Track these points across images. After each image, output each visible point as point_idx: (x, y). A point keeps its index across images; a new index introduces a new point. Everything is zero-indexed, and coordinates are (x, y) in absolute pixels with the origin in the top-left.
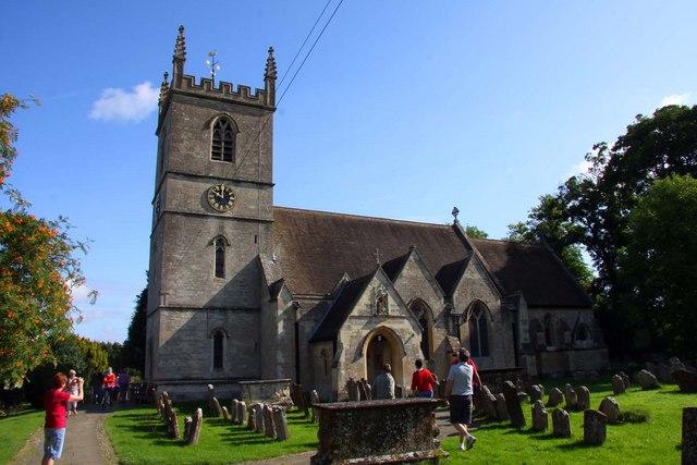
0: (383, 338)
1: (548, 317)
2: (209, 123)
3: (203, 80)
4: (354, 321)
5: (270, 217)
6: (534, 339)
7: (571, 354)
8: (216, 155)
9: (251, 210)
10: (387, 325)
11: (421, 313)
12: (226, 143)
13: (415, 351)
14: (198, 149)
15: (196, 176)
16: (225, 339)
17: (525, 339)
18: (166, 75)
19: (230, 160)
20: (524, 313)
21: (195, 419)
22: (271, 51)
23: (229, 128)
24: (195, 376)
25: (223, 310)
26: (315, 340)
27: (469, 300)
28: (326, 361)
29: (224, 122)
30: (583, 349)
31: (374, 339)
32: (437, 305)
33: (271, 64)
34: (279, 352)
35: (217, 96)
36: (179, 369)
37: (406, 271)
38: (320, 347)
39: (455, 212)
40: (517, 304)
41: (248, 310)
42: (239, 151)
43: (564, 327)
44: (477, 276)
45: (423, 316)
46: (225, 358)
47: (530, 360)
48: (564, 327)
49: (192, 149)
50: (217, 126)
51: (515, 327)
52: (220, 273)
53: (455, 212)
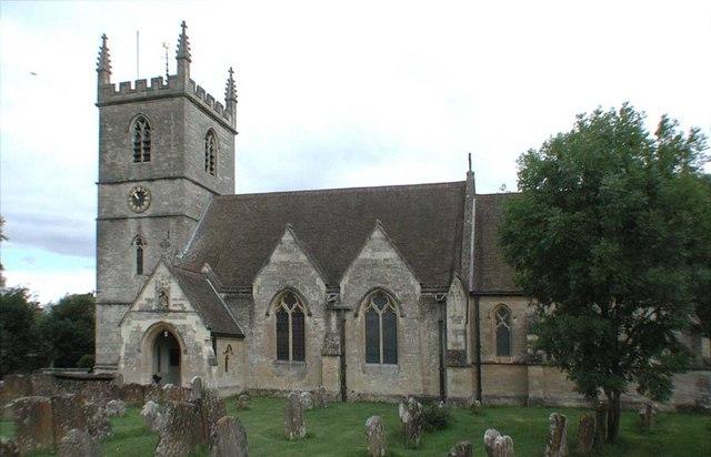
8: (137, 157)
9: (164, 206)
10: (168, 321)
27: (365, 287)
32: (315, 292)
36: (110, 356)
42: (154, 149)
44: (390, 254)
45: (297, 308)
51: (442, 325)
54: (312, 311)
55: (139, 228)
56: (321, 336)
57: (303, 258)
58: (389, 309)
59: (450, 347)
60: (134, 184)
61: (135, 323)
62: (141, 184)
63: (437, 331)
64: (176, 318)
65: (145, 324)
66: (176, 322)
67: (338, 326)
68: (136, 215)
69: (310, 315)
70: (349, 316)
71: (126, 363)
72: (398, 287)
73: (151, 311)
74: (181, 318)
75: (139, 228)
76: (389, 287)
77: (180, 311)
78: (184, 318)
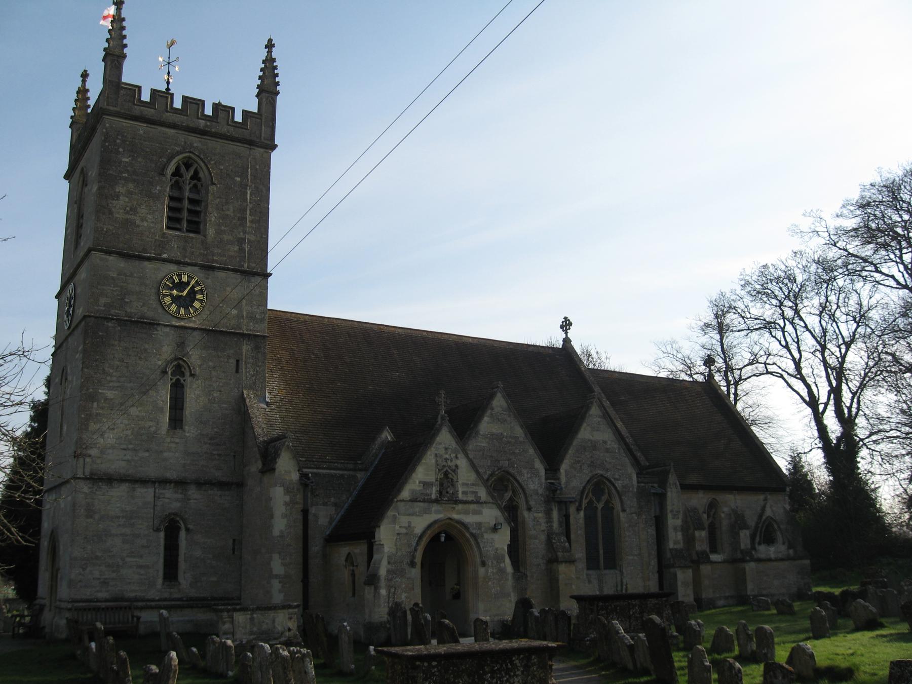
0: (449, 537)
1: (712, 506)
2: (165, 167)
3: (154, 92)
4: (401, 505)
5: (262, 329)
6: (689, 540)
7: (750, 566)
8: (174, 221)
10: (456, 516)
11: (508, 495)
12: (191, 201)
13: (500, 559)
14: (143, 211)
15: (140, 258)
16: (183, 534)
17: (676, 542)
18: (85, 75)
19: (197, 232)
20: (675, 499)
21: (166, 668)
22: (270, 45)
23: (195, 176)
24: (132, 595)
25: (180, 483)
26: (335, 537)
28: (353, 575)
29: (188, 166)
30: (770, 560)
31: (435, 538)
33: (269, 69)
34: (276, 557)
35: (177, 119)
36: (105, 583)
37: (486, 426)
38: (343, 551)
39: (566, 325)
40: (663, 483)
41: (222, 485)
42: (213, 217)
43: (738, 521)
44: (605, 436)
46: (182, 565)
47: (683, 576)
48: (738, 521)
49: (133, 210)
50: (177, 173)
51: (660, 523)
52: (176, 421)
53: (566, 325)
54: (532, 503)
55: (181, 345)
56: (543, 537)
57: (519, 432)
58: (607, 502)
59: (671, 545)
60: (173, 267)
61: (404, 520)
62: (189, 268)
63: (654, 527)
64: (466, 512)
65: (420, 524)
66: (468, 519)
67: (560, 523)
68: (175, 323)
69: (529, 509)
70: (572, 509)
71: (389, 588)
72: (617, 477)
73: (431, 501)
74: (476, 512)
75: (181, 345)
76: (608, 475)
77: (472, 502)
78: (479, 513)
